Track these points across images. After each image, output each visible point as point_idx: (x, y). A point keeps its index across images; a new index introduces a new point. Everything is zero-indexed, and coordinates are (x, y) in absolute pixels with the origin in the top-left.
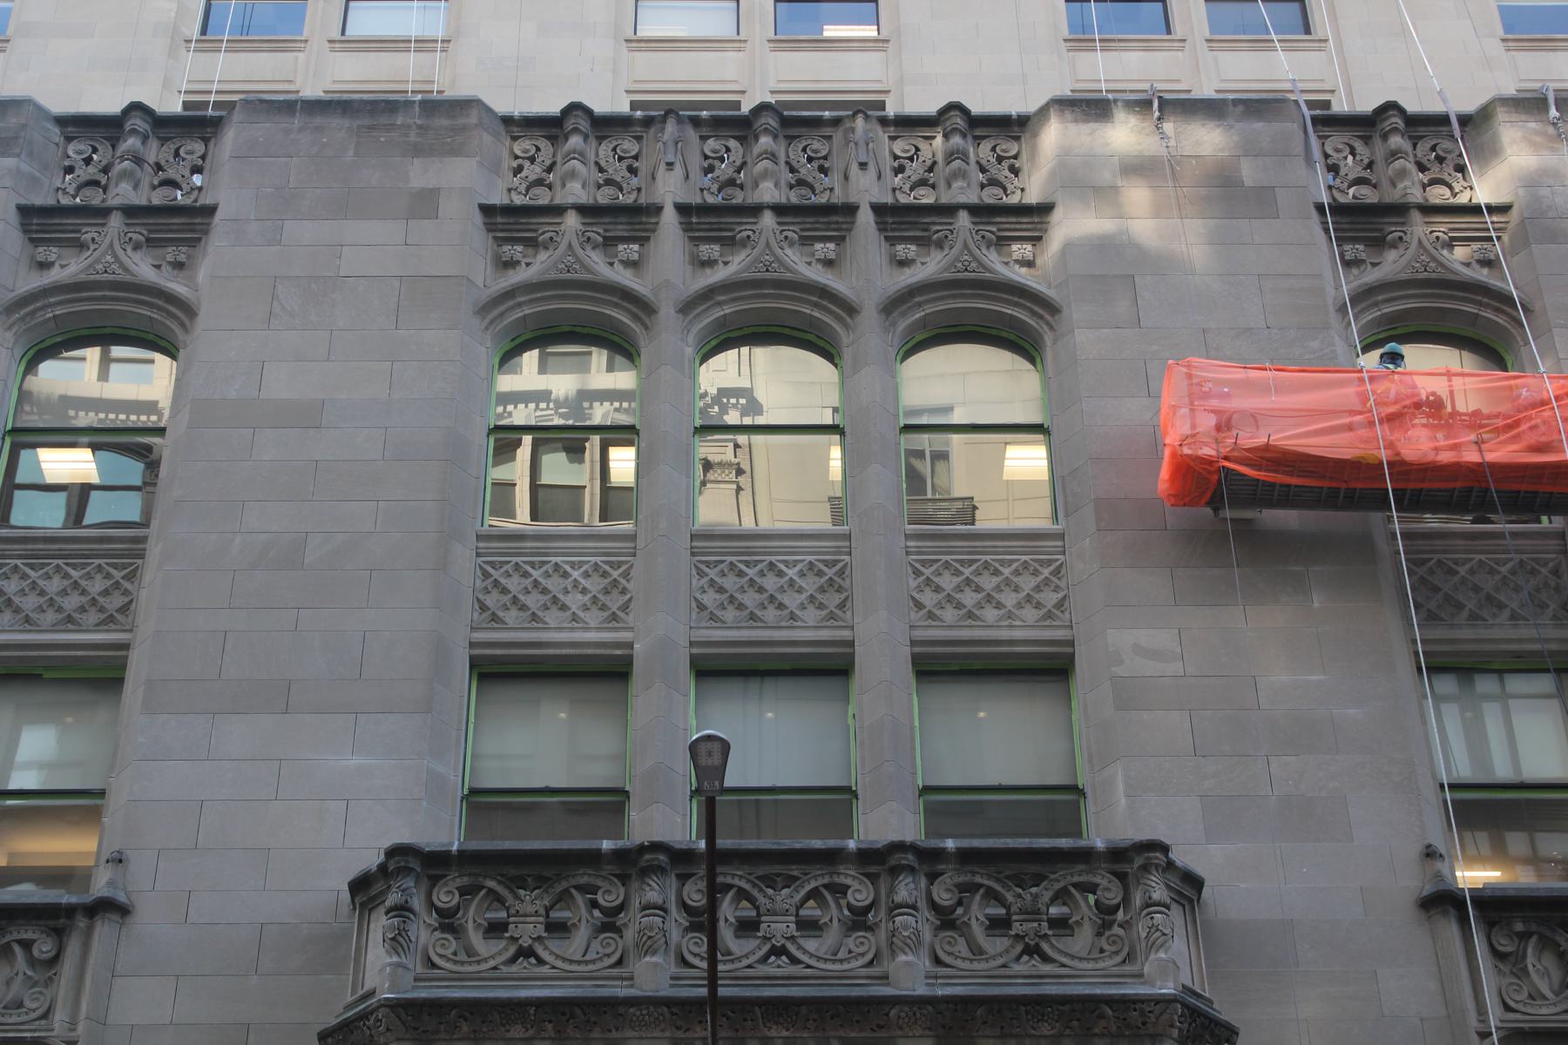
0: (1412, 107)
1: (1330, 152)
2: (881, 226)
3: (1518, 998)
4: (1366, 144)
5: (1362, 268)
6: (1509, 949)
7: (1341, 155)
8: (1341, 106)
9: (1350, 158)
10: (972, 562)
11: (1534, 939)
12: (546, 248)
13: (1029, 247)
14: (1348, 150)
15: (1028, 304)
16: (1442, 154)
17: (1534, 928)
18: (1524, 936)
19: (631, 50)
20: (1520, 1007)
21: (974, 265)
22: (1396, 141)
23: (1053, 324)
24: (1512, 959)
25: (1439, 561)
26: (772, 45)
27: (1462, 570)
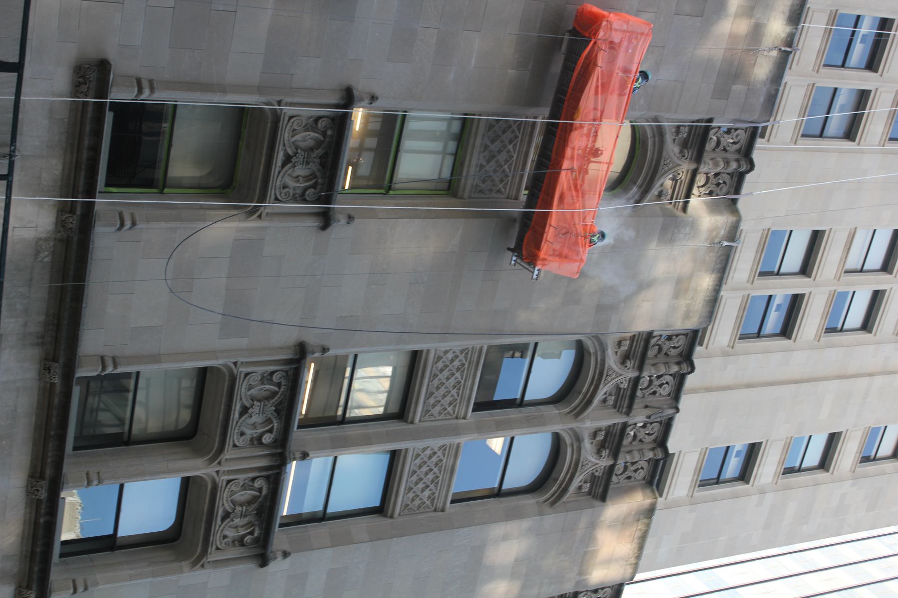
0: (749, 177)
1: (738, 132)
2: (641, 334)
3: (295, 124)
4: (736, 151)
5: (674, 134)
6: (319, 125)
7: (734, 137)
8: (698, 349)
9: (732, 141)
10: (514, 149)
11: (322, 138)
12: (680, 153)
13: (612, 403)
14: (677, 346)
15: (581, 405)
16: (638, 472)
17: (327, 140)
18: (324, 134)
19: (808, 85)
20: (290, 124)
21: (666, 169)
22: (734, 165)
23: (572, 414)
24: (314, 126)
25: (517, 137)
26: (834, 12)
27: (510, 147)
